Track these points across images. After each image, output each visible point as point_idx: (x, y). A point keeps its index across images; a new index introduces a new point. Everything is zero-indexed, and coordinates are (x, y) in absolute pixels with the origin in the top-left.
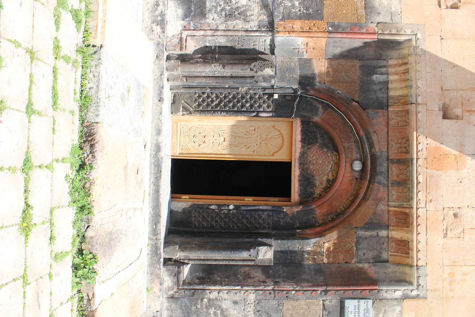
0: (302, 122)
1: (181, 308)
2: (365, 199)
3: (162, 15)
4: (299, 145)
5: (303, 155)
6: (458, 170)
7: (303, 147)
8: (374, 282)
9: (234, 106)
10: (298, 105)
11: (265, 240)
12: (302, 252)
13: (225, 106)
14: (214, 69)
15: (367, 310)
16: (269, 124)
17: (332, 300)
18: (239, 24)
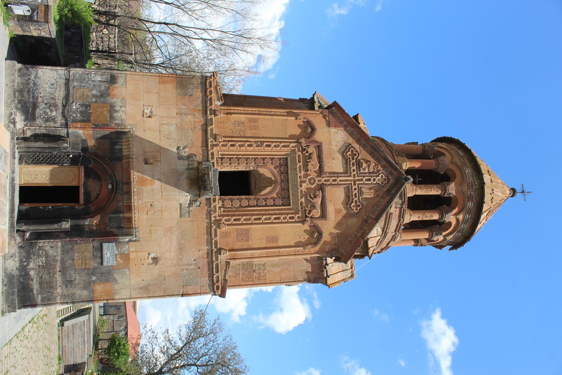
0: (85, 168)
1: (25, 251)
2: (112, 201)
3: (14, 119)
4: (83, 178)
5: (85, 183)
6: (151, 186)
7: (85, 179)
8: (116, 235)
9: (51, 161)
10: (82, 160)
11: (65, 219)
12: (84, 225)
13: (46, 160)
14: (40, 144)
15: (113, 247)
16: (69, 169)
17: (96, 244)
18: (52, 124)
